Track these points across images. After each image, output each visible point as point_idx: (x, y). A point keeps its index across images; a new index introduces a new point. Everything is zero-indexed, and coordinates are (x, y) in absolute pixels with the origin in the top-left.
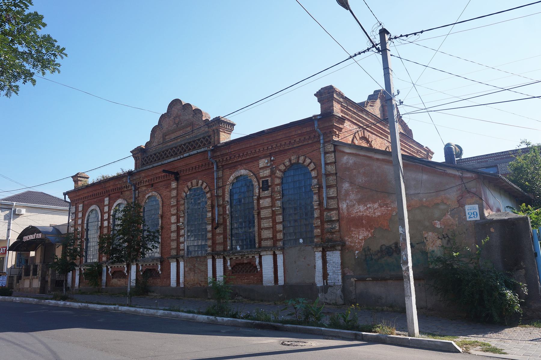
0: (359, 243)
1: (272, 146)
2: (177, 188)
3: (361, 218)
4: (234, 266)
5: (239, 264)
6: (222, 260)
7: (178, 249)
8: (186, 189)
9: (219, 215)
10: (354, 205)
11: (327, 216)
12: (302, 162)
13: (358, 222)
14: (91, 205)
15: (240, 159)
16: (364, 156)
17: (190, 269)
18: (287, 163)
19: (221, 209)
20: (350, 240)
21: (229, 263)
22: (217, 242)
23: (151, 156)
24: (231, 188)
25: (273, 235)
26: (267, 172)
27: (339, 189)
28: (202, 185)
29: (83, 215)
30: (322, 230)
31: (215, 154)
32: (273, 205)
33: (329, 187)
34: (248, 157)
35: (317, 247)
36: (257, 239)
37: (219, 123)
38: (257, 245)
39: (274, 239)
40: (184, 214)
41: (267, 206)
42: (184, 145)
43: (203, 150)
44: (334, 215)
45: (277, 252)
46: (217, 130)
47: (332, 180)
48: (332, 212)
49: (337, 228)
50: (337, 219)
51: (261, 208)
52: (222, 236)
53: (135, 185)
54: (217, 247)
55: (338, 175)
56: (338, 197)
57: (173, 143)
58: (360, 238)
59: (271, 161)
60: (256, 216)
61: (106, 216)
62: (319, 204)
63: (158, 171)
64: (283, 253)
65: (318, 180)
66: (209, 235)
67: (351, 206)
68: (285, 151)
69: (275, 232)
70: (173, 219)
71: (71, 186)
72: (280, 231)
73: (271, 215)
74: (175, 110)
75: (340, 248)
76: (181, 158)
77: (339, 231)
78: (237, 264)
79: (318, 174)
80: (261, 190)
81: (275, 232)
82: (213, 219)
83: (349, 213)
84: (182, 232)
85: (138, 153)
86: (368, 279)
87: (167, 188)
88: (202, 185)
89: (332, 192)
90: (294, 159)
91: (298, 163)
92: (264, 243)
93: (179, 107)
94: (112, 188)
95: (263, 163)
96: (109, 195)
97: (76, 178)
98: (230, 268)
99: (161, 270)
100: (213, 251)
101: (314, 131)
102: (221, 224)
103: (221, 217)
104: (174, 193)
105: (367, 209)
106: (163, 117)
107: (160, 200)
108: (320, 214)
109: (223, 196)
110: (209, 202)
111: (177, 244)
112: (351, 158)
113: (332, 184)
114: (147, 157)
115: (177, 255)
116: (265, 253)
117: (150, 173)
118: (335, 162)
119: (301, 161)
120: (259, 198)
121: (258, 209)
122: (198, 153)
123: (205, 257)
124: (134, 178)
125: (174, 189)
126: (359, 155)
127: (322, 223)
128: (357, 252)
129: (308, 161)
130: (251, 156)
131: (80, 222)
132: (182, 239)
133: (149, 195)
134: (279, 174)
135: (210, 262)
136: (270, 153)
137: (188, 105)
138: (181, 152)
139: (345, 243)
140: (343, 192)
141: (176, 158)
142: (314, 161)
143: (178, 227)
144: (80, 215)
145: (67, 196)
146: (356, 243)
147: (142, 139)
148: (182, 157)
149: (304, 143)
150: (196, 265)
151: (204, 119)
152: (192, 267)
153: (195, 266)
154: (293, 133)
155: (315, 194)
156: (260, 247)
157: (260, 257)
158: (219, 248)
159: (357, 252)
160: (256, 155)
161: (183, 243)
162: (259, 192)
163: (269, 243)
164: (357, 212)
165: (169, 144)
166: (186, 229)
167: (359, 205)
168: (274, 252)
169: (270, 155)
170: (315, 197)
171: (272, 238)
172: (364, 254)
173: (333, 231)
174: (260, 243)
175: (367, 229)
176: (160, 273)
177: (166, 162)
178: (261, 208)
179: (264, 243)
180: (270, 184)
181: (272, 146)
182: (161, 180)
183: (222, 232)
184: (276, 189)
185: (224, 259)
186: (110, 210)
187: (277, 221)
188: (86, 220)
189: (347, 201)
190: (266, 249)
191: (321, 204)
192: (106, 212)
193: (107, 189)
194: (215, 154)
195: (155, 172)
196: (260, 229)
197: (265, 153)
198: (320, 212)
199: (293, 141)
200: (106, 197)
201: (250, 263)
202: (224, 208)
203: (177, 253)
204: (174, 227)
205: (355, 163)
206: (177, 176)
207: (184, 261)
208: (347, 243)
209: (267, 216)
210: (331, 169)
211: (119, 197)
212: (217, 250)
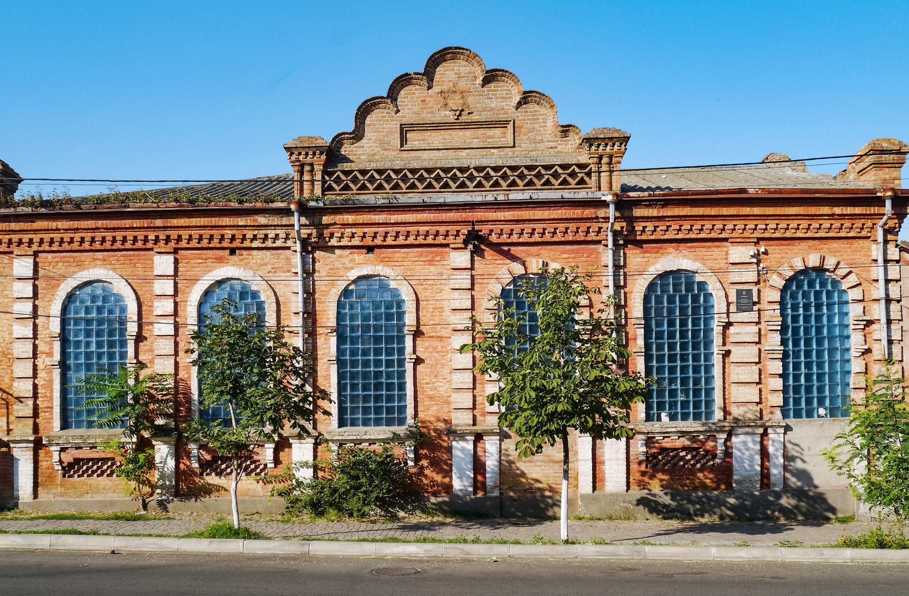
120: (729, 324)
148: (501, 198)
165: (425, 155)
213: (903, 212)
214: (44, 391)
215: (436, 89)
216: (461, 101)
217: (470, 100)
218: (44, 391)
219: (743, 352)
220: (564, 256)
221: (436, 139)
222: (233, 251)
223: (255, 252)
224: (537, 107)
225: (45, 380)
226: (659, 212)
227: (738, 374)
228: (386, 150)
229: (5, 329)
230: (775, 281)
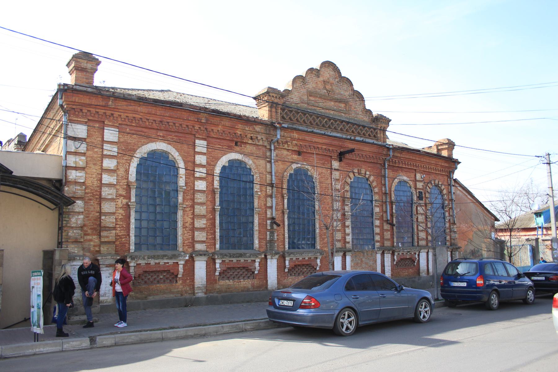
37: (381, 122)
45: (430, 250)
52: (389, 233)
117: (307, 138)
127: (450, 232)
135: (379, 256)
137: (348, 82)
148: (353, 138)
152: (359, 262)
153: (362, 261)
154: (440, 164)
174: (418, 242)
213: (454, 167)
214: (121, 223)
215: (321, 79)
217: (334, 87)
218: (121, 223)
222: (236, 144)
223: (248, 146)
225: (122, 215)
229: (94, 176)
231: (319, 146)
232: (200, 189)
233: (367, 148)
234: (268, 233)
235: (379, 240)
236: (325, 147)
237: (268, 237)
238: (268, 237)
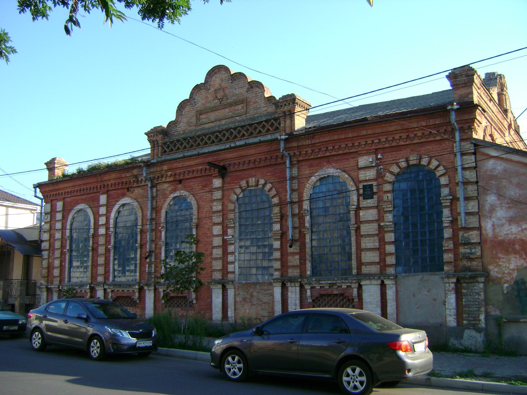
0: (509, 274)
1: (380, 140)
2: (222, 188)
3: (512, 243)
4: (317, 298)
5: (324, 295)
6: (298, 288)
7: (225, 271)
8: (238, 191)
9: (294, 228)
10: (502, 225)
11: (463, 237)
12: (425, 164)
13: (507, 246)
14: (78, 203)
15: (328, 154)
16: (519, 162)
17: (244, 299)
18: (403, 164)
19: (296, 219)
20: (496, 270)
21: (309, 293)
22: (290, 264)
23: (178, 141)
24: (311, 192)
25: (380, 259)
26: (371, 174)
27: (481, 202)
28: (264, 185)
29: (64, 218)
30: (456, 255)
31: (290, 145)
32: (380, 219)
33: (467, 199)
34: (341, 152)
35: (448, 277)
36: (354, 263)
38: (354, 271)
39: (382, 263)
40: (234, 223)
41: (371, 219)
42: (235, 129)
43: (269, 137)
44: (474, 236)
45: (386, 282)
46: (290, 111)
47: (472, 190)
48: (471, 233)
49: (479, 253)
50: (479, 241)
51: (361, 222)
52: (297, 257)
53: (152, 180)
54: (290, 271)
55: (479, 184)
56: (480, 213)
57: (212, 125)
58: (512, 267)
59: (377, 159)
60: (353, 233)
61: (102, 220)
62: (452, 222)
63: (192, 163)
64: (396, 283)
65: (450, 189)
66: (277, 255)
67: (498, 226)
68: (399, 148)
69: (383, 255)
70: (217, 230)
71: (44, 177)
72: (391, 254)
73: (377, 232)
74: (216, 81)
75: (482, 279)
76: (231, 148)
77: (481, 257)
78: (322, 296)
79: (449, 181)
80: (361, 198)
81: (383, 255)
82: (283, 234)
83: (495, 236)
84: (231, 248)
85: (156, 136)
86: (521, 320)
87: (206, 186)
88: (264, 185)
89: (473, 206)
90: (413, 160)
91: (419, 165)
92: (365, 270)
93: (223, 75)
94: (112, 182)
95: (363, 161)
96: (108, 191)
97: (51, 166)
98: (310, 300)
99: (197, 298)
100: (282, 276)
101: (449, 123)
102: (296, 241)
103: (297, 231)
104: (218, 195)
105: (522, 230)
106: (197, 88)
107: (194, 202)
108: (453, 235)
109: (300, 202)
110: (276, 210)
111: (223, 264)
112: (499, 162)
113: (471, 195)
114: (172, 142)
115: (223, 279)
116: (368, 282)
117: (179, 165)
118: (475, 168)
119: (424, 162)
120: (358, 208)
121: (356, 223)
122: (261, 142)
123: (270, 284)
124: (152, 170)
125: (217, 189)
126: (511, 161)
127: (456, 245)
128: (506, 285)
129: (435, 163)
130: (345, 151)
131: (59, 225)
132: (231, 258)
133: (176, 195)
134: (389, 177)
135: (277, 291)
136: (376, 149)
137: (241, 75)
138: (228, 139)
139: (489, 274)
140: (487, 207)
141: (223, 147)
142: (444, 163)
143: (224, 241)
144: (59, 216)
145: (38, 190)
146: (504, 273)
147: (165, 117)
148: (233, 145)
149: (430, 139)
150: (254, 294)
151: (267, 95)
152: (248, 296)
153: (252, 296)
154: (415, 125)
155: (446, 207)
156: (359, 273)
157: (360, 287)
158: (293, 273)
159: (506, 285)
160: (354, 150)
161: (233, 263)
162: (358, 200)
163: (374, 269)
164: (507, 234)
166: (237, 245)
167: (510, 224)
168: (383, 282)
169: (376, 151)
170: (446, 212)
171: (378, 263)
172: (516, 288)
173: (472, 256)
175: (522, 256)
176: (195, 302)
177: (206, 150)
178: (361, 222)
179: (365, 270)
180: (375, 190)
181: (380, 140)
182: (195, 175)
183: (298, 251)
184: (385, 198)
185: (302, 286)
186: (109, 212)
187: (387, 240)
188: (69, 223)
189: (493, 219)
190: (370, 276)
191: (454, 221)
192: (102, 215)
193: (106, 183)
194: (290, 145)
195: (187, 164)
196: (359, 250)
197: (367, 148)
198: (453, 231)
199: (413, 135)
200: (103, 194)
201: (342, 295)
202: (301, 218)
203: (223, 276)
204: (217, 241)
205: (505, 171)
206: (223, 171)
207: (235, 288)
208: (492, 273)
209: (370, 233)
210: (471, 175)
211: (123, 195)
212: (290, 274)
216: (223, 93)
219: (368, 228)
220: (268, 174)
221: (213, 116)
224: (257, 89)
226: (311, 141)
227: (365, 243)
228: (190, 126)
230: (388, 177)
231: (194, 168)
232: (102, 233)
233: (253, 151)
234: (147, 265)
235: (280, 267)
236: (200, 168)
237: (147, 269)
238: (147, 269)
